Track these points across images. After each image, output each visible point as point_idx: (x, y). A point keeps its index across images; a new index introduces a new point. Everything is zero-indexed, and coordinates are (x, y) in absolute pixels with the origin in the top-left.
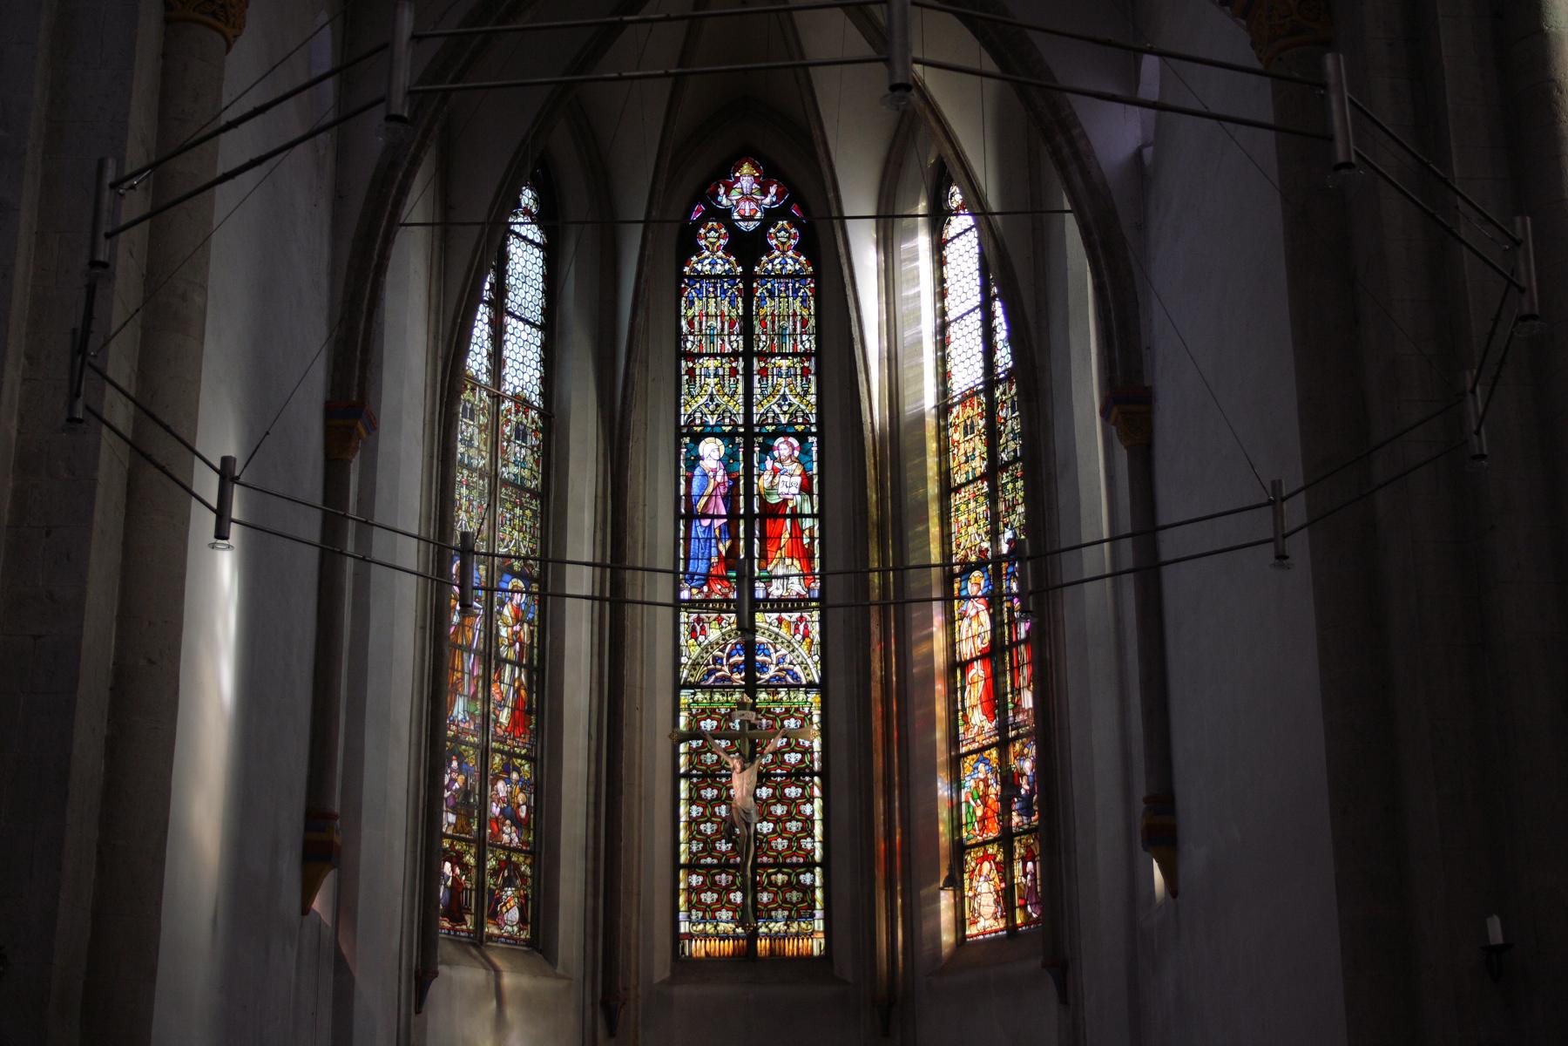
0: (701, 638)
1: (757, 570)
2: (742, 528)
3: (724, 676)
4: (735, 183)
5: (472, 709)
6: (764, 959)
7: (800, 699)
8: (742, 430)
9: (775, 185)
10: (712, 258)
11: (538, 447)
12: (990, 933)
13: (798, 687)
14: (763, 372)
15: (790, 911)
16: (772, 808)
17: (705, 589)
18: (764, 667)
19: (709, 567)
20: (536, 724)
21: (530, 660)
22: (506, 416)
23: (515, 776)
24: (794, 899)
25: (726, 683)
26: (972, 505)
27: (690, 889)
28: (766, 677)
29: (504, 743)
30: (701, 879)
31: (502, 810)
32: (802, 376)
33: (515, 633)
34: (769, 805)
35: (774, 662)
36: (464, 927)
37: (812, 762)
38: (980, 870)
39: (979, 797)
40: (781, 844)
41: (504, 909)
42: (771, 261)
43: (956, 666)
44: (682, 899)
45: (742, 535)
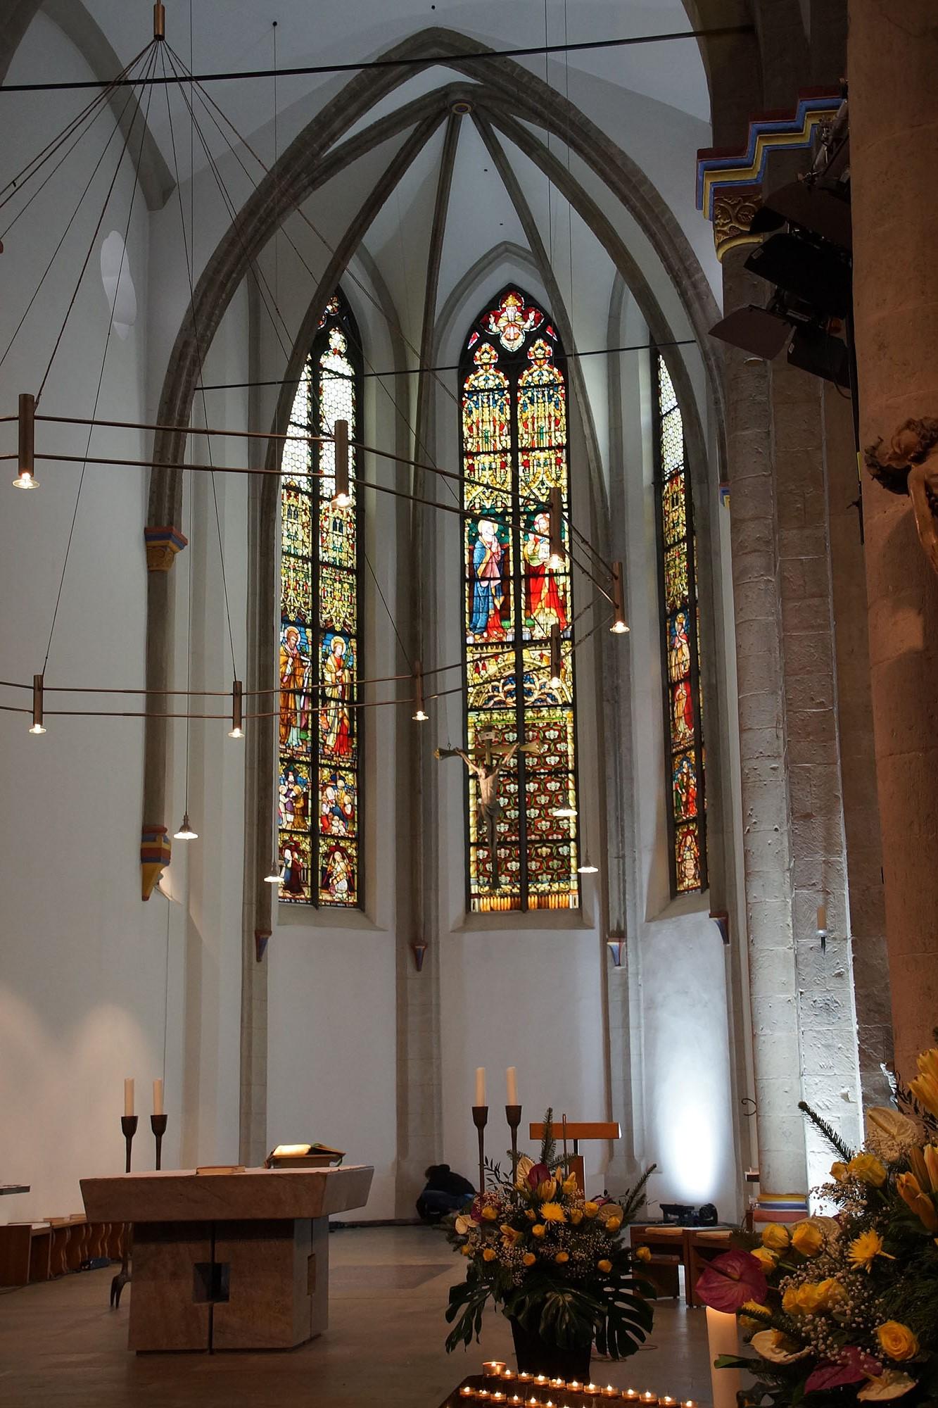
0: (483, 672)
1: (523, 618)
2: (512, 586)
3: (500, 701)
4: (502, 313)
5: (303, 736)
7: (558, 715)
8: (510, 510)
9: (534, 312)
10: (486, 377)
11: (353, 535)
12: (692, 889)
13: (555, 706)
14: (526, 464)
15: (552, 875)
16: (538, 799)
17: (485, 635)
18: (530, 692)
19: (487, 619)
20: (357, 744)
21: (352, 696)
22: (325, 514)
23: (340, 783)
24: (555, 867)
25: (502, 706)
26: (677, 561)
27: (478, 861)
28: (532, 699)
29: (331, 759)
30: (486, 853)
31: (331, 810)
32: (556, 465)
33: (337, 677)
34: (535, 797)
35: (538, 688)
36: (303, 896)
37: (567, 762)
38: (685, 841)
39: (684, 787)
40: (544, 825)
41: (335, 882)
42: (531, 374)
44: (472, 868)
45: (512, 592)
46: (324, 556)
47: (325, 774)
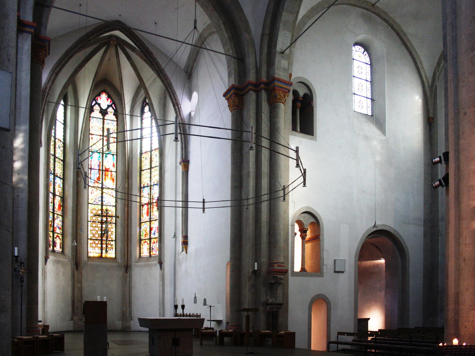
6: (104, 258)
43: (141, 205)
47: (56, 215)
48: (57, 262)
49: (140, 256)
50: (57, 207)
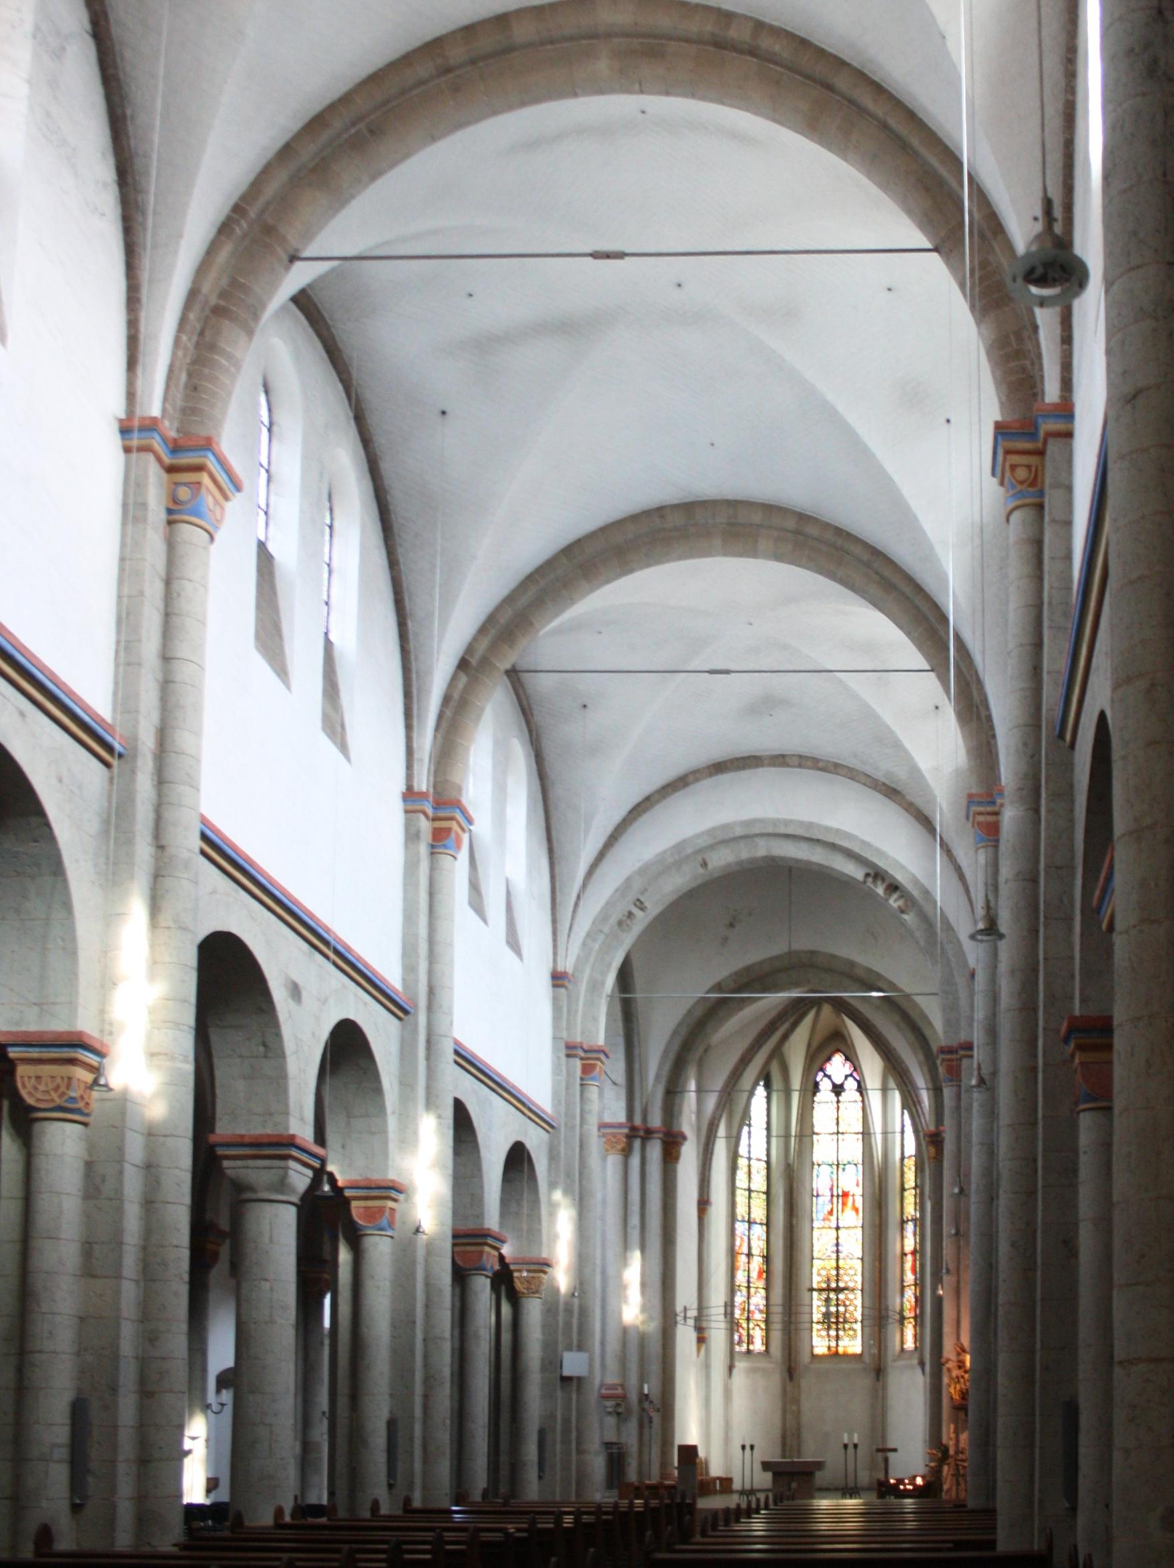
27: (818, 1330)
46: (753, 1188)
48: (753, 1370)
49: (902, 1349)
50: (754, 1275)
